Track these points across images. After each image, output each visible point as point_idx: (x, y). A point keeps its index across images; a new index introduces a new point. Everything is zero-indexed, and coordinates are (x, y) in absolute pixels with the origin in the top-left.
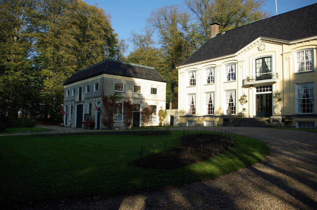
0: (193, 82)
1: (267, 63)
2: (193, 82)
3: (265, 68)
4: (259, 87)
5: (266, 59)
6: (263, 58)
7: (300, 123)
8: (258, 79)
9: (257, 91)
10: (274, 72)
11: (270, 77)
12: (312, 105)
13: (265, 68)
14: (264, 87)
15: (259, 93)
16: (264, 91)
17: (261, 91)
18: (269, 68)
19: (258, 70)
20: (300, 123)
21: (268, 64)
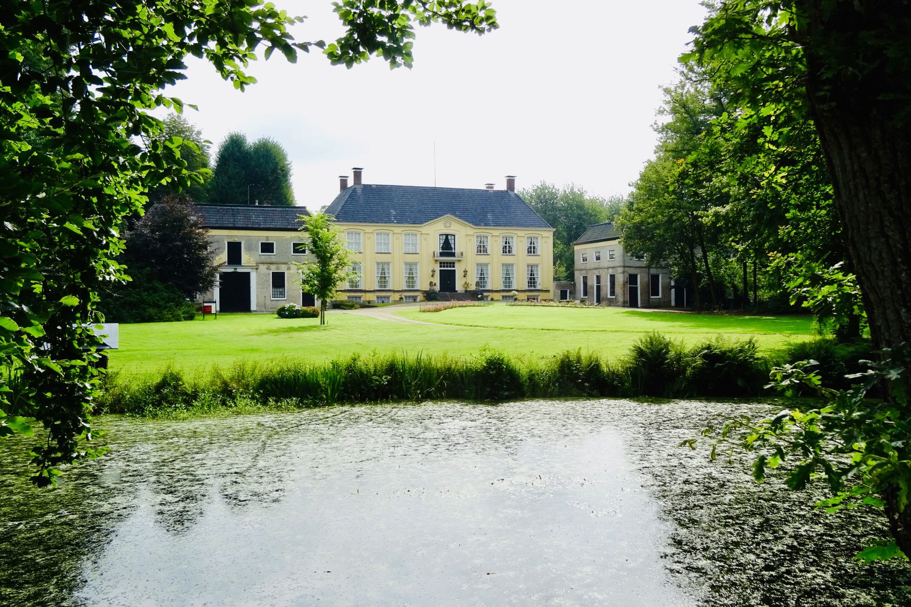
4: (442, 264)
6: (447, 235)
9: (441, 267)
11: (453, 255)
14: (447, 263)
15: (443, 268)
16: (447, 267)
17: (444, 267)
18: (453, 246)
21: (452, 242)
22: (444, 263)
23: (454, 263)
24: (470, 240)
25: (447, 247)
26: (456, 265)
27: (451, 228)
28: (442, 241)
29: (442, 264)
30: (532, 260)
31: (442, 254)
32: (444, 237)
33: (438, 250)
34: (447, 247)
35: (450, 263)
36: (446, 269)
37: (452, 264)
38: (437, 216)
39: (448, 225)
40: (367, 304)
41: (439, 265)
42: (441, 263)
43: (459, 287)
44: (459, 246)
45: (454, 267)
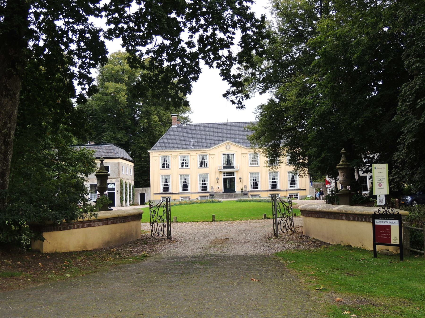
0: (165, 165)
1: (231, 158)
2: (165, 165)
3: (229, 162)
4: (225, 174)
5: (230, 156)
6: (228, 155)
7: (251, 195)
8: (224, 167)
9: (224, 176)
10: (235, 165)
11: (233, 167)
12: (258, 185)
13: (229, 162)
14: (229, 173)
15: (226, 177)
16: (229, 176)
17: (227, 176)
18: (233, 162)
19: (224, 162)
20: (251, 195)
21: (231, 158)
22: (227, 173)
23: (234, 173)
24: (244, 157)
25: (229, 164)
26: (235, 174)
27: (231, 150)
28: (226, 159)
29: (225, 174)
30: (255, 169)
31: (224, 167)
32: (227, 156)
33: (221, 164)
34: (229, 164)
35: (231, 173)
36: (228, 177)
37: (232, 174)
38: (223, 141)
39: (228, 147)
40: (136, 204)
41: (223, 175)
42: (224, 173)
43: (238, 189)
44: (237, 162)
45: (234, 175)
